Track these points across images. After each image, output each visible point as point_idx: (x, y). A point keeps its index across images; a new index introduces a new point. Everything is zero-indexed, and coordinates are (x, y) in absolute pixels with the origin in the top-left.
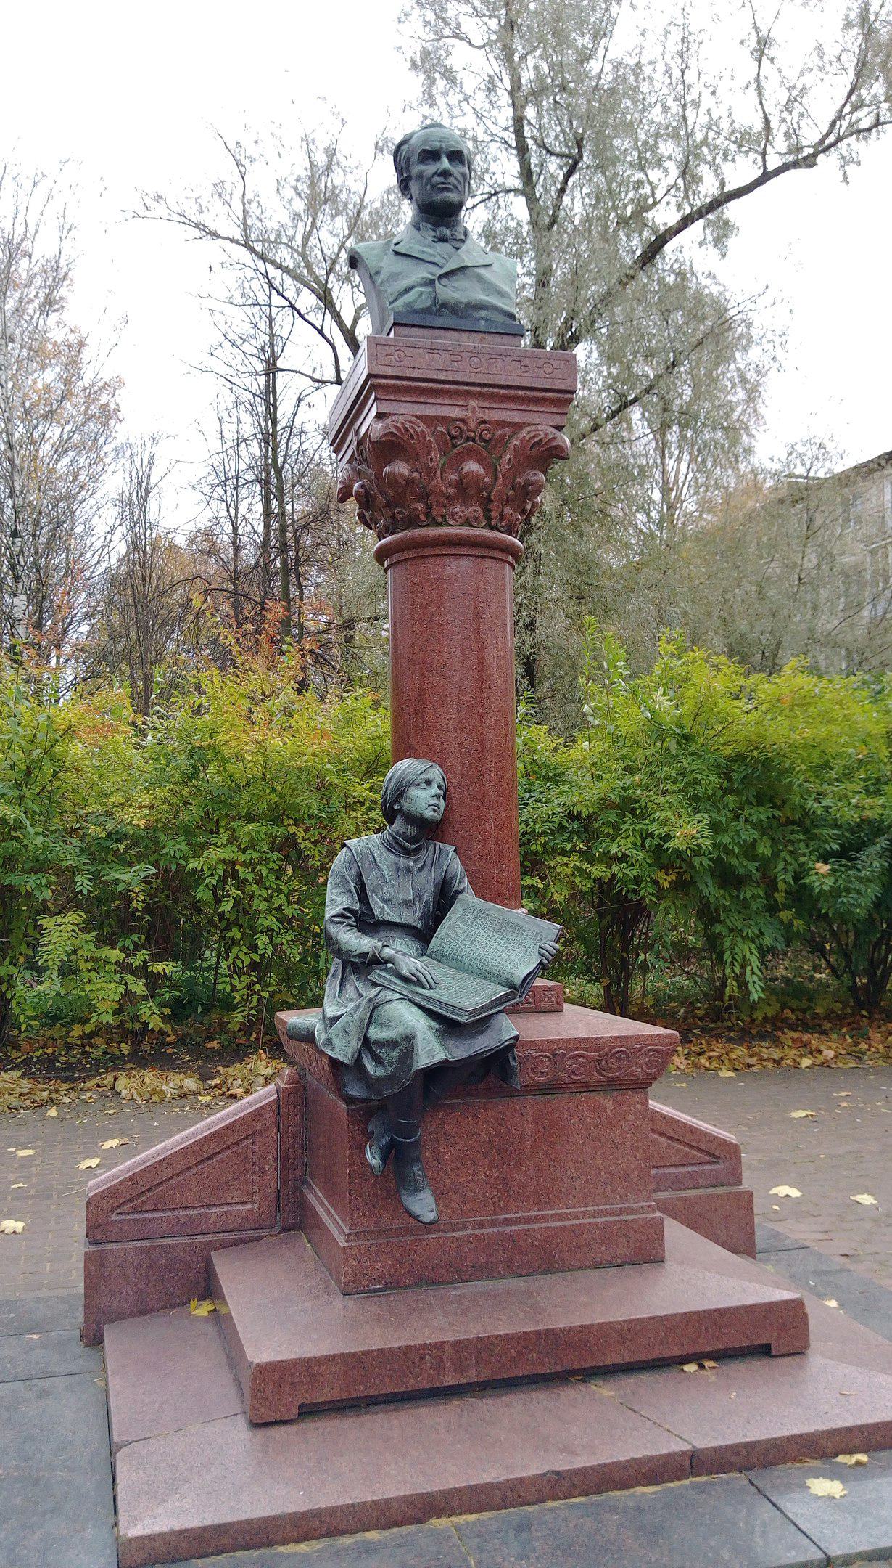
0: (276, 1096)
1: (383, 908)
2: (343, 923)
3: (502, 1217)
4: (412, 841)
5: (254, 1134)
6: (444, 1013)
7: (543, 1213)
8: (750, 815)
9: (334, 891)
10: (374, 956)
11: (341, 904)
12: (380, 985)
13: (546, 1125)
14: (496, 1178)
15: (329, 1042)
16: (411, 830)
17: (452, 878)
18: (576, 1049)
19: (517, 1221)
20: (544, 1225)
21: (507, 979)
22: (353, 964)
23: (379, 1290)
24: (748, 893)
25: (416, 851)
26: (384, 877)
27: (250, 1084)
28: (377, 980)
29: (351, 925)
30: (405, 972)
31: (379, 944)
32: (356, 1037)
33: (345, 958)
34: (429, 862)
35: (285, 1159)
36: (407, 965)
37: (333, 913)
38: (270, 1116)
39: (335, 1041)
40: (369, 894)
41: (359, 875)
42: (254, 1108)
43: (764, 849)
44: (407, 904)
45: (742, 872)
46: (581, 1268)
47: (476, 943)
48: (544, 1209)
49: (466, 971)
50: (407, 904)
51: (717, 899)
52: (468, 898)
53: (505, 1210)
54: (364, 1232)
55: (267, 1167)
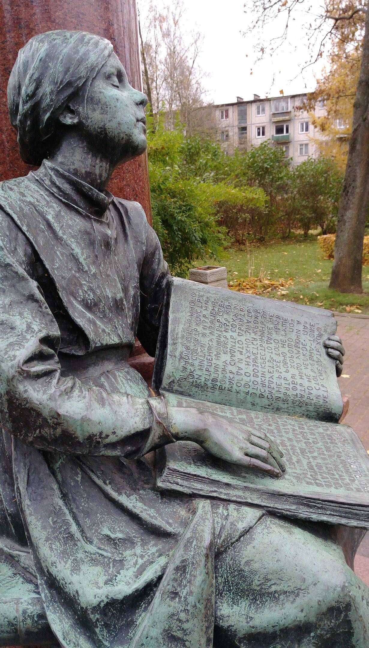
26: (75, 259)
47: (237, 354)
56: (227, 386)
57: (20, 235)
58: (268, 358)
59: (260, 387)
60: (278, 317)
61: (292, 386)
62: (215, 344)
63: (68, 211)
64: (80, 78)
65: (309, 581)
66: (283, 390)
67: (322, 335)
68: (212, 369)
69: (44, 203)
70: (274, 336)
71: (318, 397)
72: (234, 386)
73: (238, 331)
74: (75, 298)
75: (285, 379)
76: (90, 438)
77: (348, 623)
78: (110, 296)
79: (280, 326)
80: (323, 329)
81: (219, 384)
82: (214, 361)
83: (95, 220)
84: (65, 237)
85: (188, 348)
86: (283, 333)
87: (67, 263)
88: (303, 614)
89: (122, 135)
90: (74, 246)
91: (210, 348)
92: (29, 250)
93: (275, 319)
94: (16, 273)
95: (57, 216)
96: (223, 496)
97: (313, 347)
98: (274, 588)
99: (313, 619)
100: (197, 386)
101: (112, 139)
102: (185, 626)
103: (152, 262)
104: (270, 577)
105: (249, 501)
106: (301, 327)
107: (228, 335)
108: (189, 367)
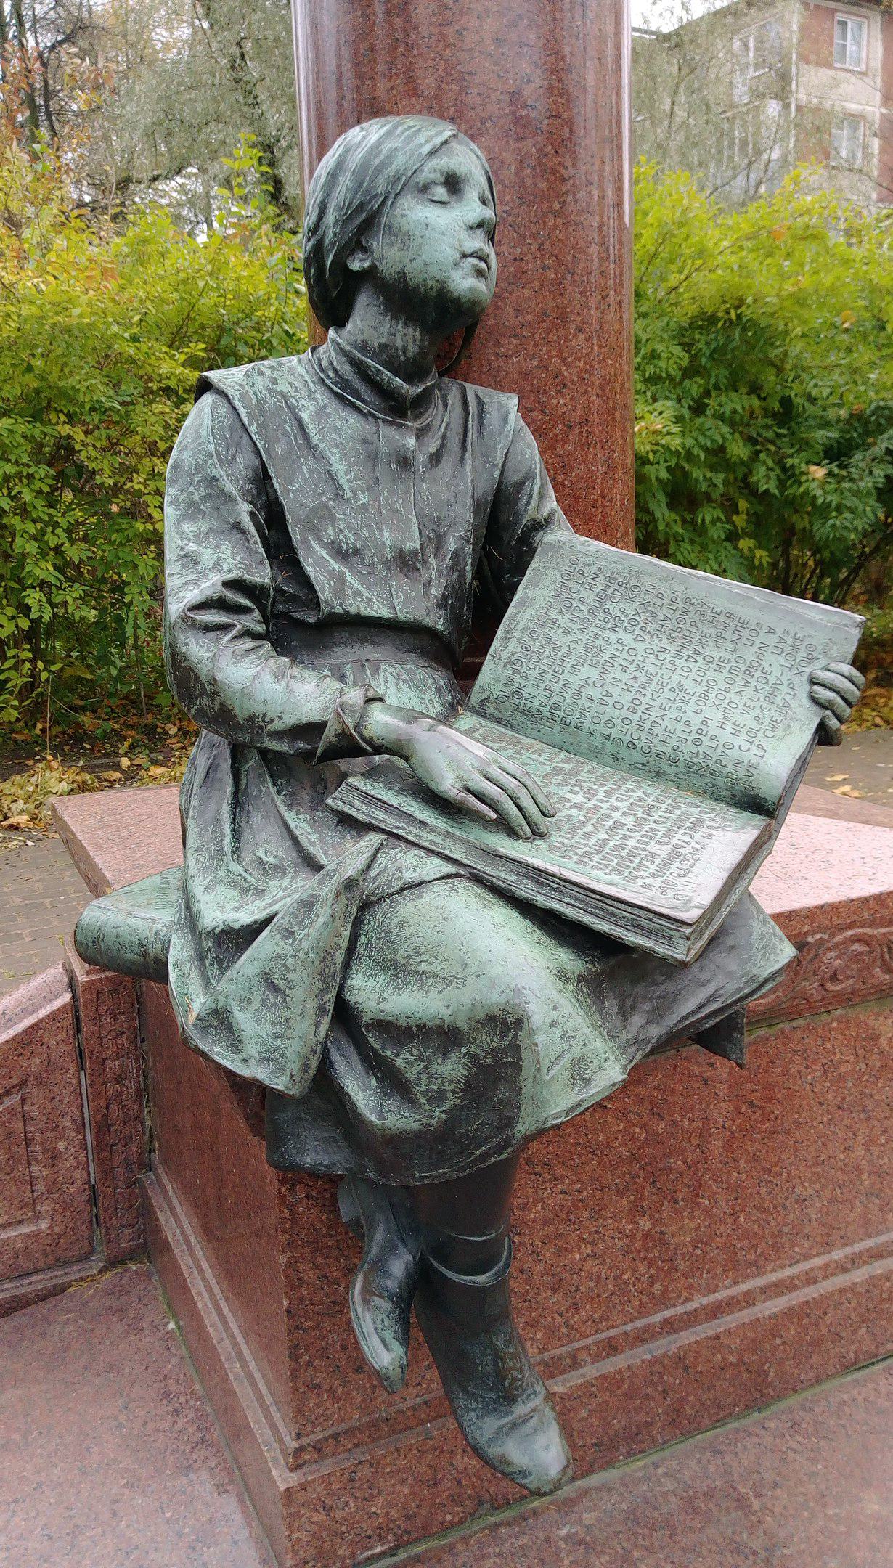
0: (67, 997)
1: (341, 578)
2: (224, 628)
3: (657, 1318)
4: (412, 372)
5: (23, 1083)
6: (603, 926)
7: (744, 1287)
8: (720, 405)
9: (188, 527)
10: (344, 735)
11: (216, 566)
12: (362, 828)
13: (756, 1097)
14: (646, 1236)
15: (219, 1020)
16: (406, 338)
17: (520, 485)
18: (851, 926)
19: (691, 1319)
20: (746, 1315)
21: (732, 783)
22: (264, 753)
23: (382, 1555)
24: (708, 514)
25: (421, 402)
26: (333, 480)
27: (37, 807)
28: (359, 811)
29: (249, 634)
30: (449, 784)
31: (355, 696)
32: (311, 1005)
33: (243, 738)
34: (454, 441)
35: (103, 1128)
36: (454, 762)
37: (193, 595)
38: (58, 1043)
39: (243, 1019)
40: (296, 536)
41: (262, 479)
42: (20, 1027)
43: (739, 450)
44: (406, 563)
45: (704, 487)
46: (818, 1381)
47: (616, 672)
48: (746, 1277)
49: (595, 754)
50: (406, 563)
51: (667, 525)
52: (561, 535)
53: (663, 1301)
54: (335, 1436)
55: (62, 1145)
56: (575, 719)
57: (245, 438)
58: (673, 684)
59: (632, 729)
60: (730, 616)
61: (694, 736)
62: (580, 648)
63: (340, 407)
64: (376, 196)
65: (472, 969)
66: (674, 742)
67: (816, 659)
68: (556, 689)
69: (304, 393)
70: (710, 649)
71: (738, 763)
72: (587, 723)
73: (637, 631)
74: (319, 538)
75: (687, 724)
76: (251, 719)
77: (516, 1048)
78: (388, 543)
79: (728, 634)
80: (820, 648)
81: (561, 714)
82: (566, 676)
83: (385, 421)
84: (322, 445)
85: (526, 648)
86: (731, 646)
87: (316, 485)
88: (450, 1012)
89: (430, 283)
90: (333, 460)
91: (566, 655)
92: (257, 462)
93: (722, 618)
94: (223, 490)
95: (321, 412)
96: (410, 838)
97: (784, 679)
98: (423, 967)
99: (463, 1024)
100: (525, 712)
101: (416, 290)
102: (291, 976)
103: (516, 502)
104: (422, 950)
105: (447, 852)
106: (772, 640)
107: (613, 637)
108: (518, 680)
